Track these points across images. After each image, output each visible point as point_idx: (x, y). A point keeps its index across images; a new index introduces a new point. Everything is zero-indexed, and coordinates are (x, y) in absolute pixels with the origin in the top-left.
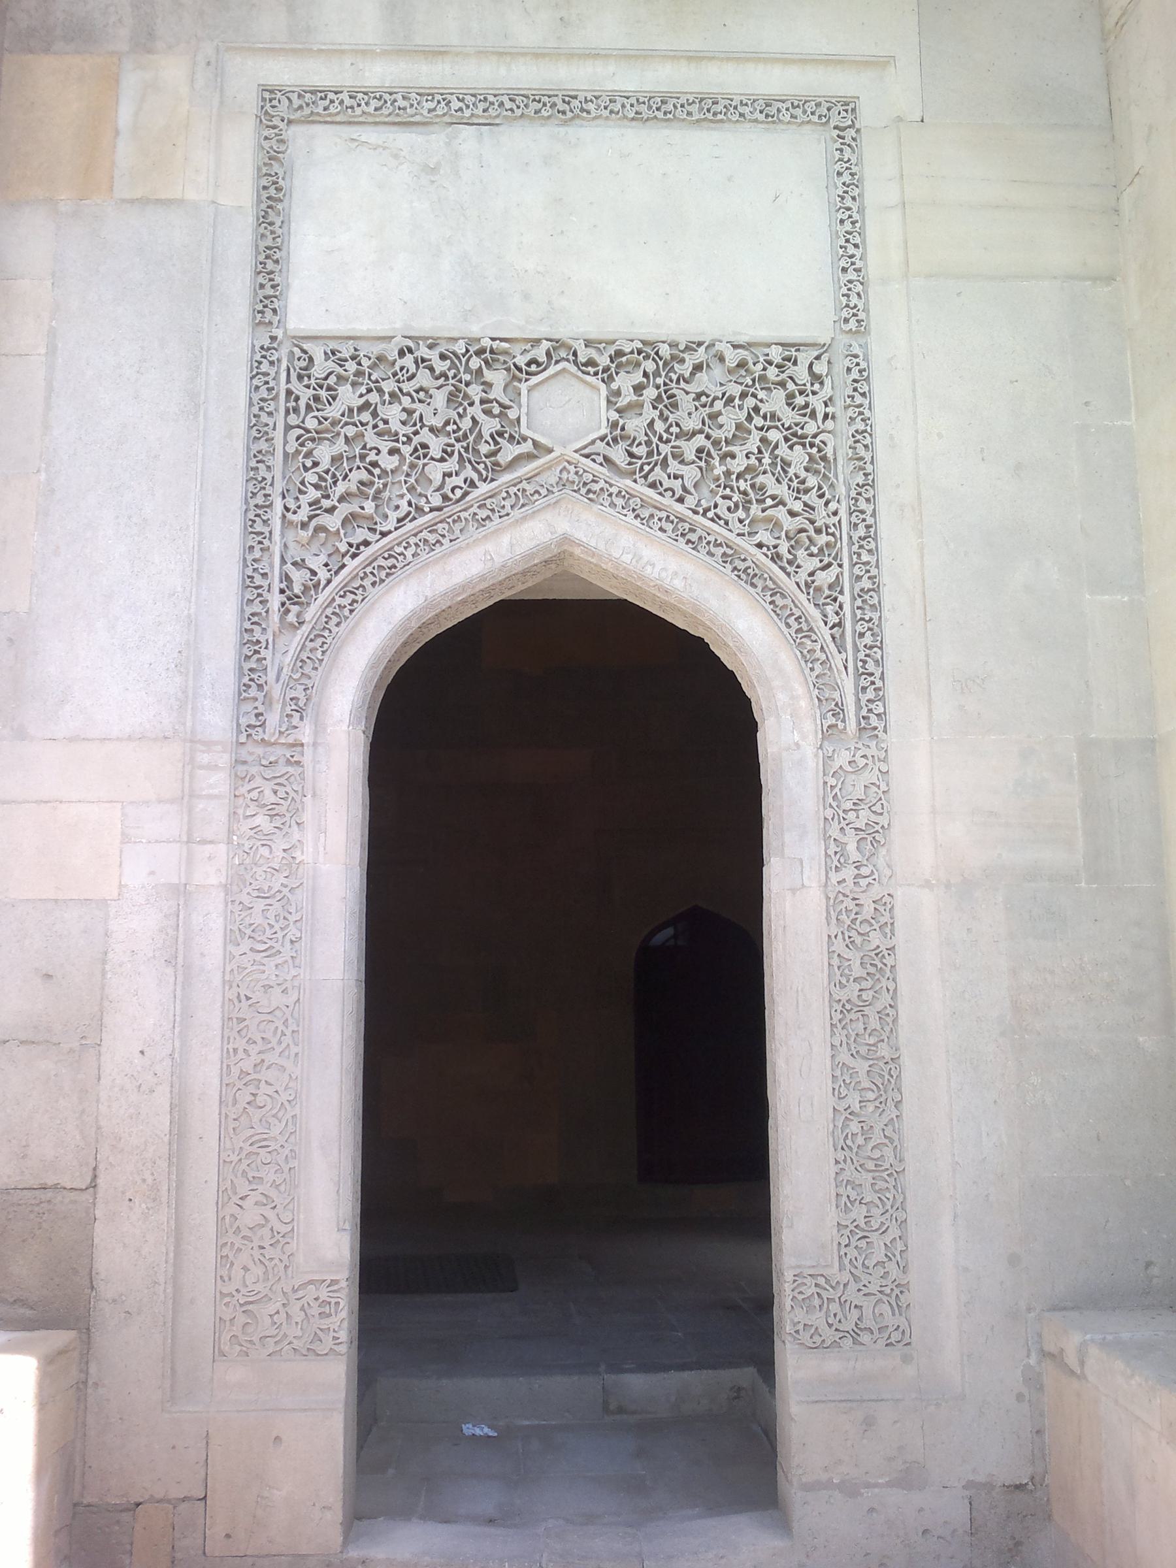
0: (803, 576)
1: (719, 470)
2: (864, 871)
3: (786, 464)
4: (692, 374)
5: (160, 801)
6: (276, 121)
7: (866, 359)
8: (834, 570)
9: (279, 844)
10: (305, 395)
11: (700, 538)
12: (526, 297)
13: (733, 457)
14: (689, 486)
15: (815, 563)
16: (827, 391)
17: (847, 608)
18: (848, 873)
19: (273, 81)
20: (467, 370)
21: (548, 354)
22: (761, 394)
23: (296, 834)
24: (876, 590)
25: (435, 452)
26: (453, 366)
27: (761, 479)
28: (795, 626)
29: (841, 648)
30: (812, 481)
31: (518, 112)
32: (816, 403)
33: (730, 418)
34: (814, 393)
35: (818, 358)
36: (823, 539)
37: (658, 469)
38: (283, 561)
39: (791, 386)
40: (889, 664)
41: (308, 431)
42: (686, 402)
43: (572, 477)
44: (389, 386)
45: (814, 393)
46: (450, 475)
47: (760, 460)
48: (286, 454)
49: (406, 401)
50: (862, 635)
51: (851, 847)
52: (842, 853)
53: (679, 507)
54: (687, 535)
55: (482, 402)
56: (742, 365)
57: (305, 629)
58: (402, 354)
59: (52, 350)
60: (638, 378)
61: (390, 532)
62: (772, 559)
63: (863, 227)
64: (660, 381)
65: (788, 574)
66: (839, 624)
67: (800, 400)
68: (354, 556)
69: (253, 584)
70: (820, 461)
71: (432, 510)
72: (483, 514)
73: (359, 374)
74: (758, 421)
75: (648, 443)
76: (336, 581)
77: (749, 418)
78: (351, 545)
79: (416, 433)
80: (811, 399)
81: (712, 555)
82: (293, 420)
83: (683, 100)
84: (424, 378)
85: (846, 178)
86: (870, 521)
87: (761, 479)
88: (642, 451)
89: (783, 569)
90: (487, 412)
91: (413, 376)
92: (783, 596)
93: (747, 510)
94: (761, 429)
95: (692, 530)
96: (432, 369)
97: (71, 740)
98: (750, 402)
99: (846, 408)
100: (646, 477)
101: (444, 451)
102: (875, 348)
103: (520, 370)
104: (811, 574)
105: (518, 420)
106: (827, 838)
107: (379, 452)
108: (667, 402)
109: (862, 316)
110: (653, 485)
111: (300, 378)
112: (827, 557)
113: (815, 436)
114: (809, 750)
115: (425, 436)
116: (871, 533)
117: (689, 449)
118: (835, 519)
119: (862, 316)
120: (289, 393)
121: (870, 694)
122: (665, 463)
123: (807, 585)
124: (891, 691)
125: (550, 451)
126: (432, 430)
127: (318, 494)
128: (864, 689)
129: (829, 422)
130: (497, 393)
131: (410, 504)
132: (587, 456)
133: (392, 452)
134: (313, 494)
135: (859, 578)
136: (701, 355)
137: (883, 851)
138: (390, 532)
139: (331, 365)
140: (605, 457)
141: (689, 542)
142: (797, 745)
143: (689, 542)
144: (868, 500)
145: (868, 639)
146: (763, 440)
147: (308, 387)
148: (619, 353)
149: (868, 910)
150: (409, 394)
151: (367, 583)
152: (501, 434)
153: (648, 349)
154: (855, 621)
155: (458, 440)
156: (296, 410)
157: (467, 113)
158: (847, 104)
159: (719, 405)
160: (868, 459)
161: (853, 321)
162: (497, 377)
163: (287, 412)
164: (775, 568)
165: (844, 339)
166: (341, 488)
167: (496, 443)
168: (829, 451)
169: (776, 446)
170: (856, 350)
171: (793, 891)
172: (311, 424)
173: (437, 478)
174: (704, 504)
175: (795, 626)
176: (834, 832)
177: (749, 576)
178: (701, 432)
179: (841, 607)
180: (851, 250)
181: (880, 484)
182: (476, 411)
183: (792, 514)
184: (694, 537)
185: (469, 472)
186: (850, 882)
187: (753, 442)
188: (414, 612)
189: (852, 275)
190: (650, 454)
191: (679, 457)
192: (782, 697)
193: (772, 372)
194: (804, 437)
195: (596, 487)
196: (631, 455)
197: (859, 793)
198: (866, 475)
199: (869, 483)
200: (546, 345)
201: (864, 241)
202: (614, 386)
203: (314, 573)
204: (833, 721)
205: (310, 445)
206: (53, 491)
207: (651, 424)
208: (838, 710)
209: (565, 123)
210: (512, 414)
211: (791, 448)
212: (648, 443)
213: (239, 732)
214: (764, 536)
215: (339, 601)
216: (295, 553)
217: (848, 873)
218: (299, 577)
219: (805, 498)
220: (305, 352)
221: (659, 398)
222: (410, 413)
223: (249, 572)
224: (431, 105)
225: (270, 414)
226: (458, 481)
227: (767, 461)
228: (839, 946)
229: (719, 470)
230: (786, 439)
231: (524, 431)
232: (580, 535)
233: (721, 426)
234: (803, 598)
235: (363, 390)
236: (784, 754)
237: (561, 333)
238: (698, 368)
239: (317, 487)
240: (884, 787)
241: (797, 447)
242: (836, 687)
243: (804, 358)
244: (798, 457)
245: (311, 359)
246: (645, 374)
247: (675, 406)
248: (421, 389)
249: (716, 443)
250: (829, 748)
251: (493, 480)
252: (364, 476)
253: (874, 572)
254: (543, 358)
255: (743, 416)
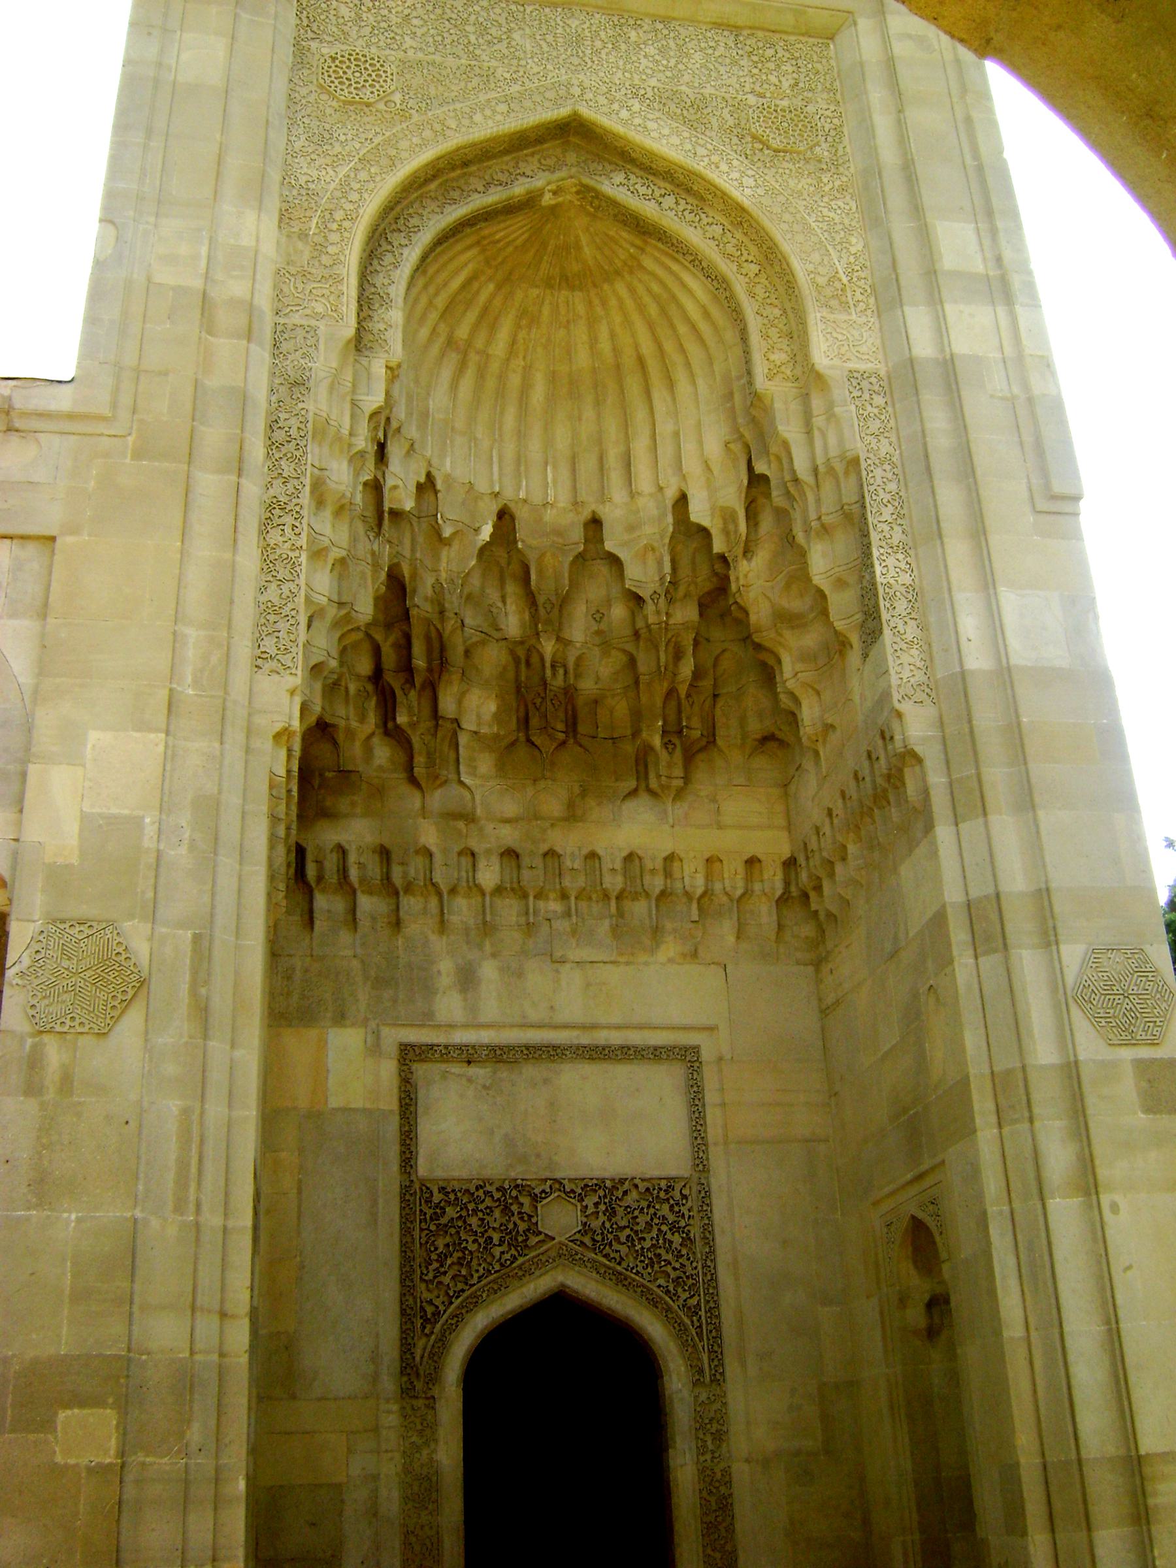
0: (681, 1302)
1: (638, 1247)
2: (717, 1455)
3: (671, 1242)
4: (623, 1195)
5: (366, 1431)
6: (407, 1062)
7: (708, 1186)
8: (696, 1298)
9: (425, 1452)
10: (429, 1212)
11: (630, 1283)
12: (538, 1156)
13: (644, 1239)
14: (623, 1255)
15: (687, 1295)
16: (689, 1204)
17: (703, 1318)
18: (708, 1456)
19: (405, 1040)
20: (511, 1197)
21: (551, 1187)
22: (657, 1207)
23: (433, 1445)
24: (718, 1307)
25: (496, 1241)
26: (504, 1195)
27: (658, 1251)
28: (678, 1328)
29: (701, 1340)
30: (684, 1252)
31: (531, 1056)
32: (684, 1210)
33: (642, 1220)
34: (683, 1205)
35: (684, 1186)
36: (691, 1281)
37: (607, 1247)
38: (422, 1302)
39: (672, 1202)
40: (725, 1346)
41: (431, 1231)
42: (620, 1211)
43: (565, 1252)
44: (471, 1206)
45: (683, 1205)
46: (502, 1253)
47: (658, 1241)
48: (421, 1244)
49: (480, 1215)
50: (711, 1331)
51: (709, 1443)
52: (705, 1446)
53: (619, 1268)
54: (621, 1280)
55: (519, 1213)
56: (648, 1189)
57: (433, 1337)
58: (477, 1189)
59: (300, 1192)
60: (597, 1200)
61: (474, 1285)
62: (666, 1294)
63: (705, 1115)
64: (606, 1200)
65: (674, 1301)
66: (700, 1327)
67: (676, 1209)
68: (457, 1297)
69: (404, 1313)
70: (688, 1240)
71: (496, 1272)
72: (520, 1273)
73: (457, 1199)
74: (656, 1221)
75: (602, 1234)
76: (450, 1310)
77: (652, 1219)
78: (455, 1292)
79: (486, 1231)
80: (682, 1208)
81: (636, 1292)
82: (424, 1226)
83: (613, 1048)
84: (488, 1202)
85: (695, 1089)
86: (713, 1271)
87: (658, 1251)
88: (599, 1238)
89: (671, 1298)
90: (522, 1219)
91: (484, 1200)
92: (672, 1313)
93: (652, 1267)
94: (657, 1225)
95: (626, 1279)
96: (492, 1196)
97: (319, 1399)
98: (652, 1211)
99: (699, 1211)
100: (601, 1252)
101: (500, 1240)
102: (713, 1180)
103: (536, 1195)
104: (685, 1301)
105: (537, 1223)
106: (697, 1438)
107: (467, 1242)
108: (611, 1213)
109: (705, 1163)
110: (606, 1256)
111: (426, 1202)
112: (693, 1290)
113: (684, 1227)
114: (686, 1393)
115: (491, 1233)
116: (714, 1278)
117: (623, 1236)
118: (695, 1272)
119: (705, 1163)
120: (421, 1211)
121: (716, 1362)
122: (611, 1245)
123: (683, 1306)
124: (727, 1361)
125: (554, 1239)
126: (494, 1229)
127: (438, 1265)
128: (713, 1360)
129: (691, 1220)
130: (527, 1208)
131: (484, 1269)
132: (572, 1241)
133: (475, 1241)
134: (436, 1265)
135: (708, 1302)
136: (626, 1186)
137: (724, 1445)
138: (474, 1285)
139: (441, 1196)
140: (581, 1242)
141: (624, 1285)
142: (681, 1390)
143: (624, 1285)
144: (711, 1260)
145: (714, 1334)
146: (659, 1230)
147: (430, 1208)
148: (586, 1186)
149: (719, 1475)
150: (481, 1211)
151: (464, 1311)
152: (529, 1230)
153: (600, 1184)
154: (707, 1324)
155: (507, 1234)
156: (425, 1219)
157: (505, 1056)
158: (695, 1048)
159: (636, 1213)
160: (711, 1239)
161: (701, 1166)
162: (525, 1200)
163: (421, 1222)
164: (667, 1299)
165: (697, 1175)
166: (449, 1261)
167: (526, 1236)
168: (692, 1235)
169: (665, 1234)
170: (703, 1181)
171: (682, 1466)
172: (433, 1228)
173: (497, 1255)
174: (631, 1265)
175: (678, 1328)
176: (701, 1436)
177: (654, 1302)
178: (628, 1227)
179: (700, 1317)
180: (699, 1128)
181: (718, 1252)
182: (516, 1218)
183: (675, 1269)
184: (626, 1283)
185: (513, 1252)
186: (709, 1461)
187: (654, 1233)
188: (486, 1326)
189: (699, 1141)
190: (603, 1240)
191: (617, 1239)
192: (672, 1366)
193: (662, 1194)
194: (679, 1228)
195: (577, 1257)
196: (593, 1240)
197: (712, 1414)
198: (710, 1247)
199: (712, 1252)
200: (549, 1183)
201: (705, 1123)
202: (584, 1204)
203: (437, 1307)
204: (697, 1377)
205: (433, 1239)
206: (304, 1267)
207: (603, 1223)
208: (701, 1371)
209: (553, 1061)
210: (534, 1220)
211: (673, 1234)
212: (602, 1234)
213: (402, 1392)
214: (661, 1281)
215: (450, 1321)
216: (427, 1295)
217: (708, 1456)
218: (430, 1310)
219: (680, 1260)
220: (428, 1188)
221: (607, 1209)
222: (482, 1220)
223: (404, 1307)
224: (486, 1052)
225: (412, 1222)
226: (507, 1256)
227: (661, 1241)
228: (705, 1494)
229: (638, 1247)
230: (670, 1229)
231: (540, 1229)
232: (569, 1283)
233: (638, 1224)
234: (681, 1313)
235: (458, 1209)
236: (674, 1396)
237: (558, 1175)
238: (625, 1193)
239: (437, 1261)
240: (724, 1411)
241: (676, 1234)
242: (699, 1359)
243: (678, 1187)
244: (677, 1239)
245: (431, 1192)
246: (600, 1197)
247: (615, 1212)
248: (487, 1207)
249: (636, 1232)
250: (697, 1391)
251: (526, 1255)
252: (460, 1254)
253: (715, 1298)
254: (548, 1190)
255: (648, 1218)
